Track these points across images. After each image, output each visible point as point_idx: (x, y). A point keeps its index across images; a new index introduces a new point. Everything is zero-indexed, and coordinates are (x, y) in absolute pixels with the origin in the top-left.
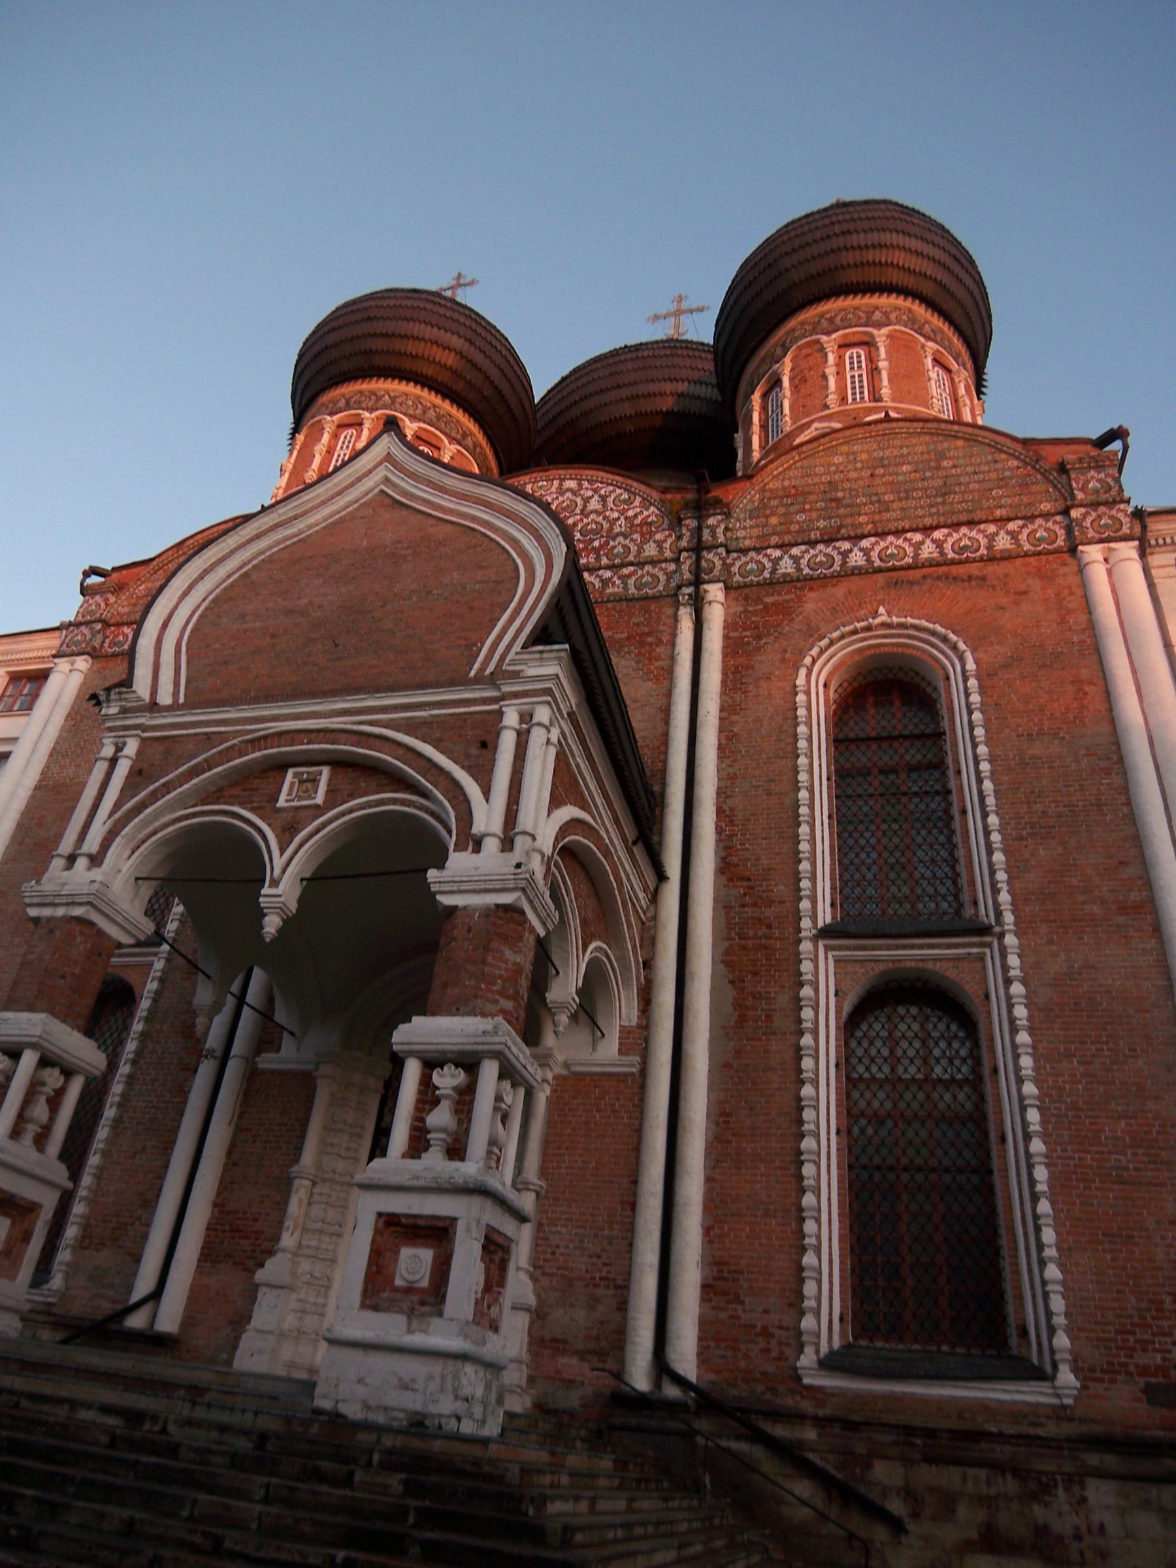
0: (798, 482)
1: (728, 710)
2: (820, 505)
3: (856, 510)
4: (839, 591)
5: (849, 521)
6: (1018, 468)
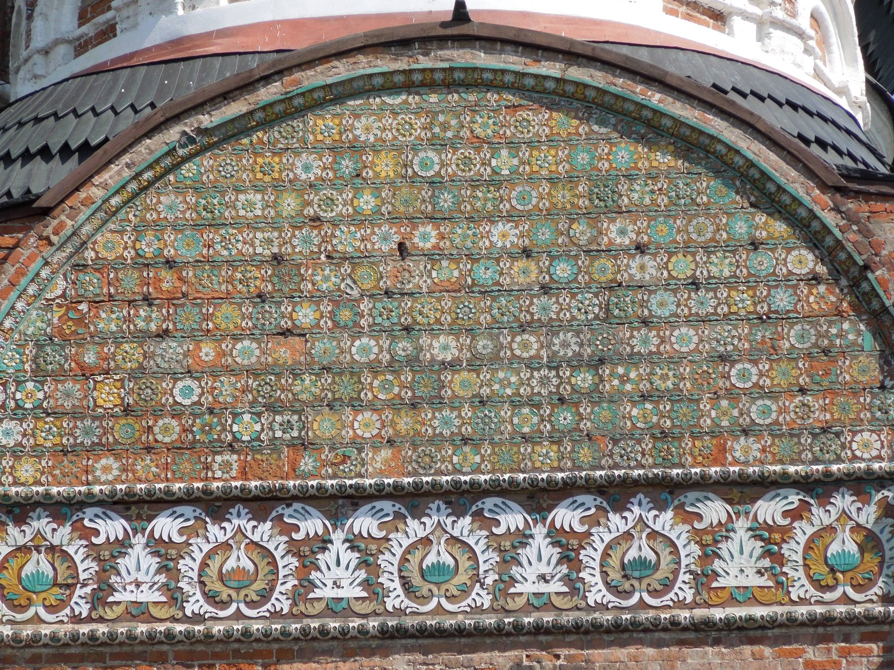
0: (177, 246)
2: (246, 352)
3: (345, 388)
5: (323, 426)
6: (815, 279)
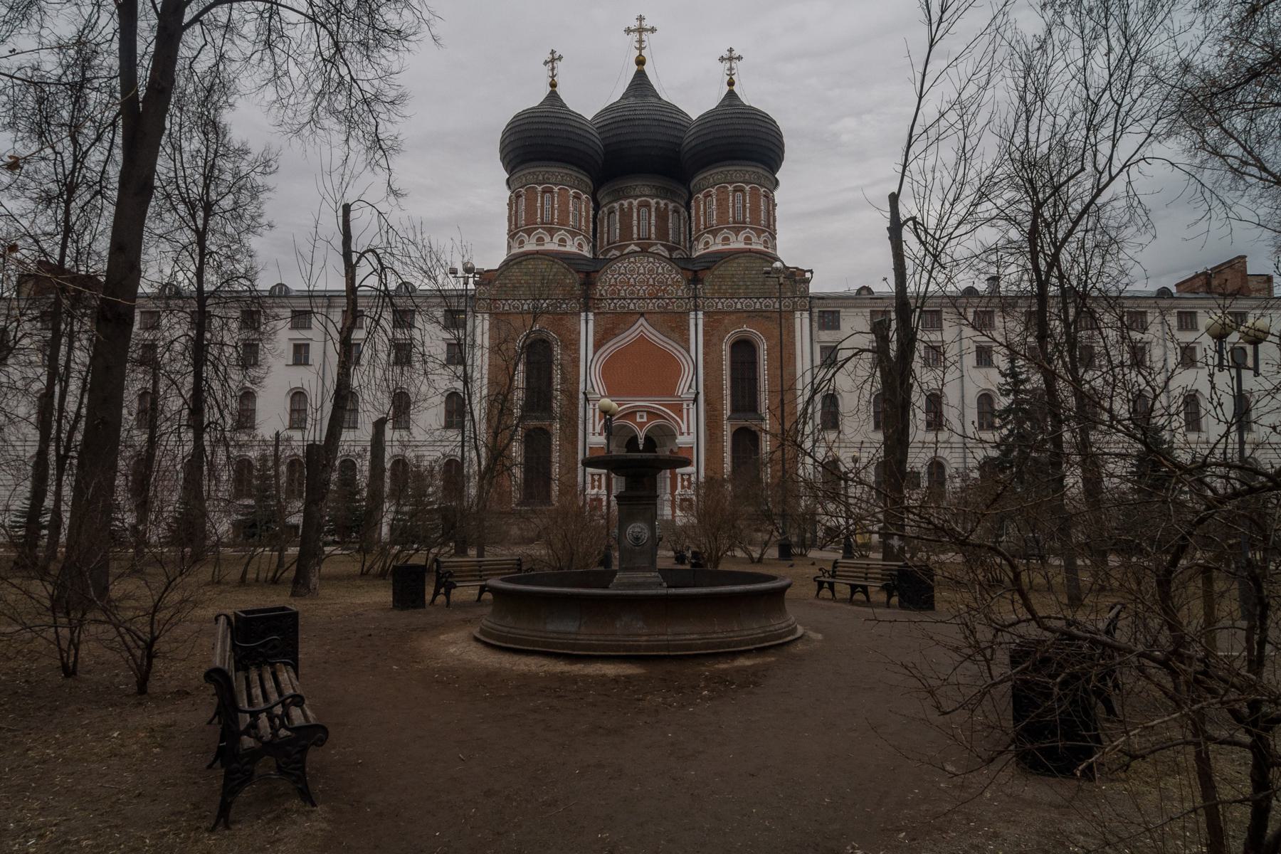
1: (705, 354)
4: (733, 317)
